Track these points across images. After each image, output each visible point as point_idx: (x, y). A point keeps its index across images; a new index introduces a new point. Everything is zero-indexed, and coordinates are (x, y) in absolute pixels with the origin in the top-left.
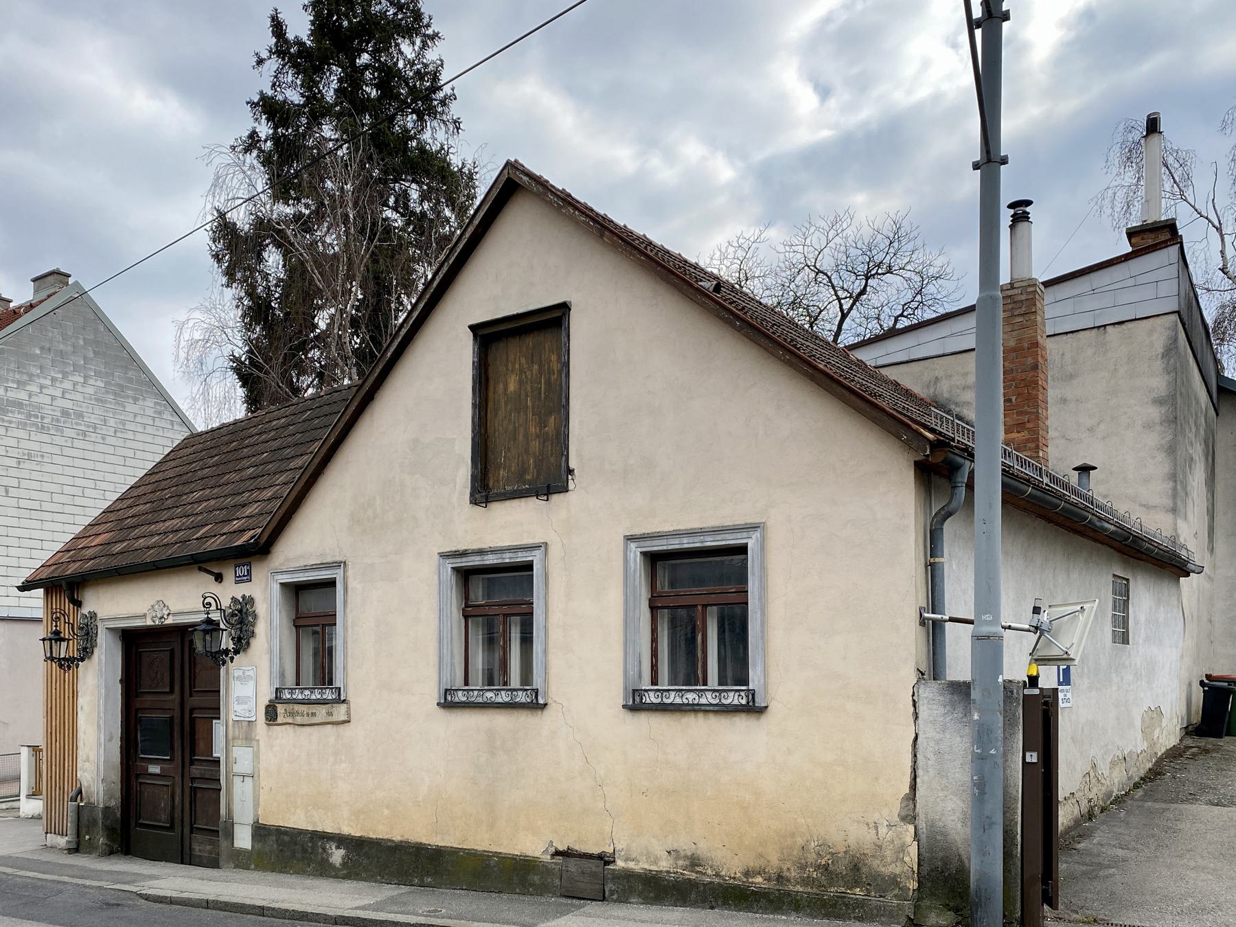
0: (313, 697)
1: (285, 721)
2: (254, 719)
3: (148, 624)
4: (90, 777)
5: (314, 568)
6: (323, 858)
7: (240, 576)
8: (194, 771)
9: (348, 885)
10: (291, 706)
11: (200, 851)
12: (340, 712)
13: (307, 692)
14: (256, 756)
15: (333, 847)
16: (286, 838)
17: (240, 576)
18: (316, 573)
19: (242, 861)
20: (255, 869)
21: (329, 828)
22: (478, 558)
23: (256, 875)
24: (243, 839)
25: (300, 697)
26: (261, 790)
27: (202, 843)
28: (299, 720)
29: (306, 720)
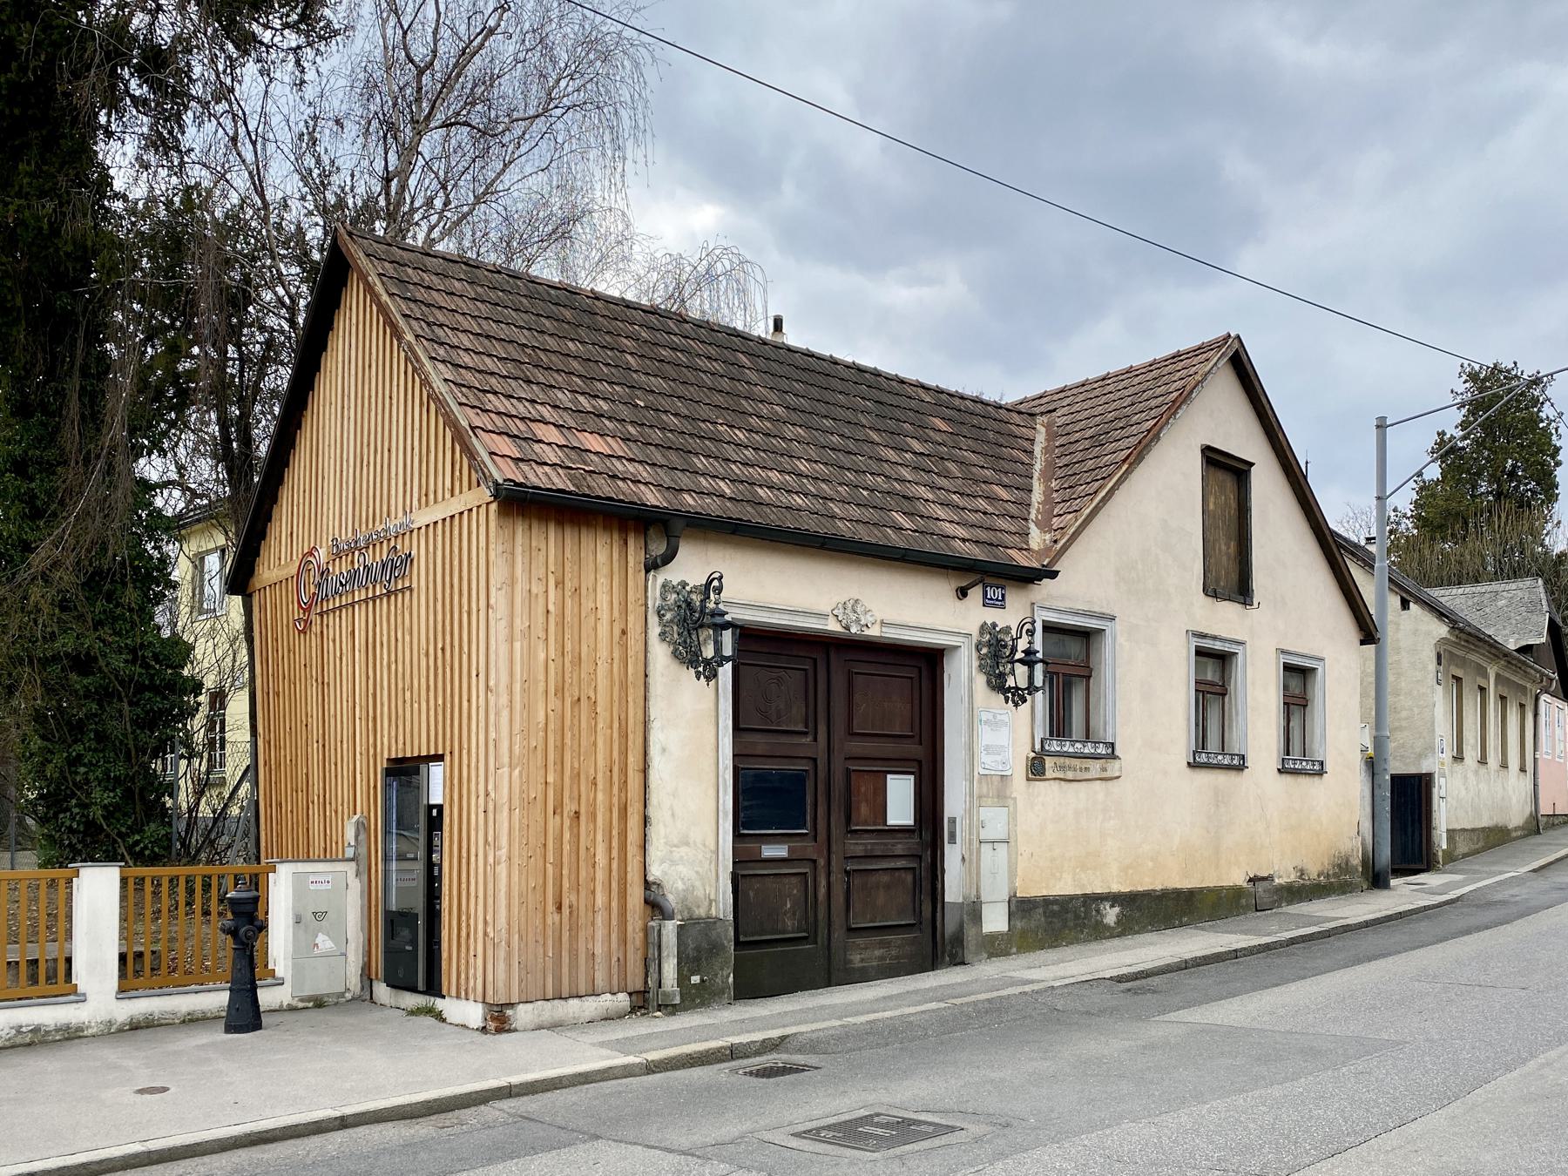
0: (1086, 751)
1: (1054, 776)
2: (1009, 773)
3: (829, 628)
4: (694, 876)
5: (1085, 614)
6: (1097, 921)
7: (991, 599)
8: (852, 848)
9: (1128, 941)
10: (1062, 759)
11: (862, 960)
12: (1113, 768)
13: (1078, 745)
14: (1013, 819)
15: (1108, 907)
16: (1056, 908)
17: (991, 599)
18: (1087, 620)
19: (996, 947)
20: (1018, 952)
21: (1099, 890)
22: (1211, 642)
23: (1148, 937)
24: (995, 921)
25: (1071, 750)
26: (1020, 857)
27: (866, 948)
28: (1070, 775)
29: (1079, 775)
